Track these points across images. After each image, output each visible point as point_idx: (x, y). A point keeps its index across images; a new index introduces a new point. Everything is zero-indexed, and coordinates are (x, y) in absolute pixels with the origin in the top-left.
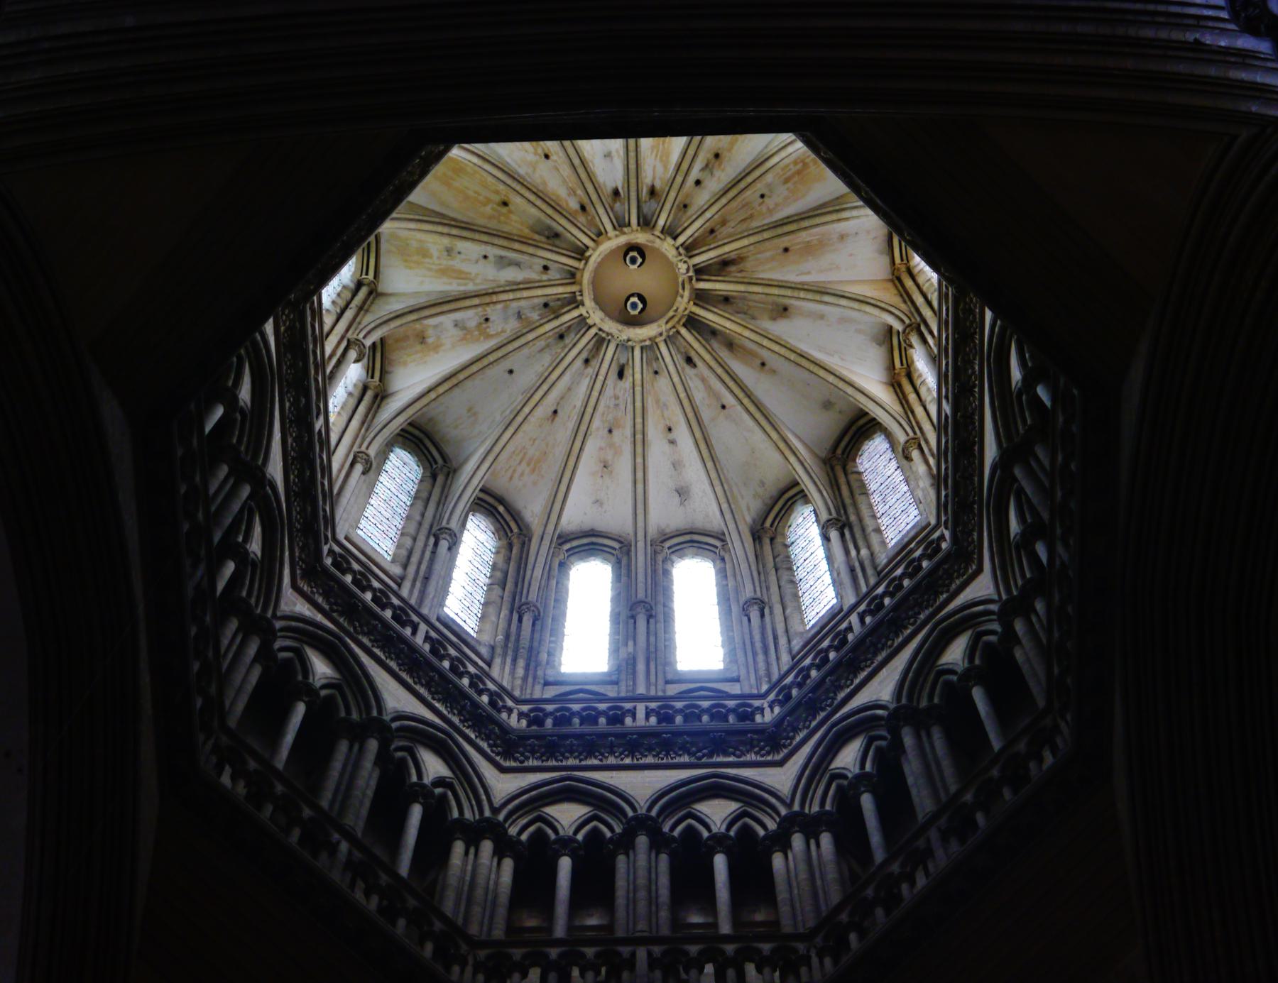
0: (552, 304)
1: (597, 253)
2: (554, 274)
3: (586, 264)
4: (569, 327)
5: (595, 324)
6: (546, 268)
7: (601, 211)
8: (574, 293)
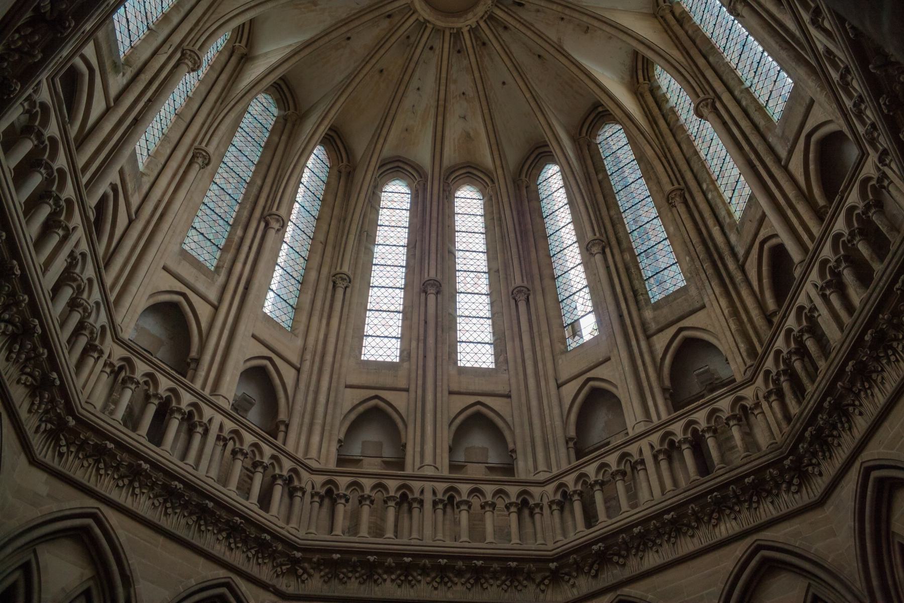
0: (459, 48)
1: (422, 13)
2: (437, 45)
3: (429, 22)
4: (477, 38)
5: (477, 22)
6: (431, 48)
7: (389, 8)
8: (451, 34)
